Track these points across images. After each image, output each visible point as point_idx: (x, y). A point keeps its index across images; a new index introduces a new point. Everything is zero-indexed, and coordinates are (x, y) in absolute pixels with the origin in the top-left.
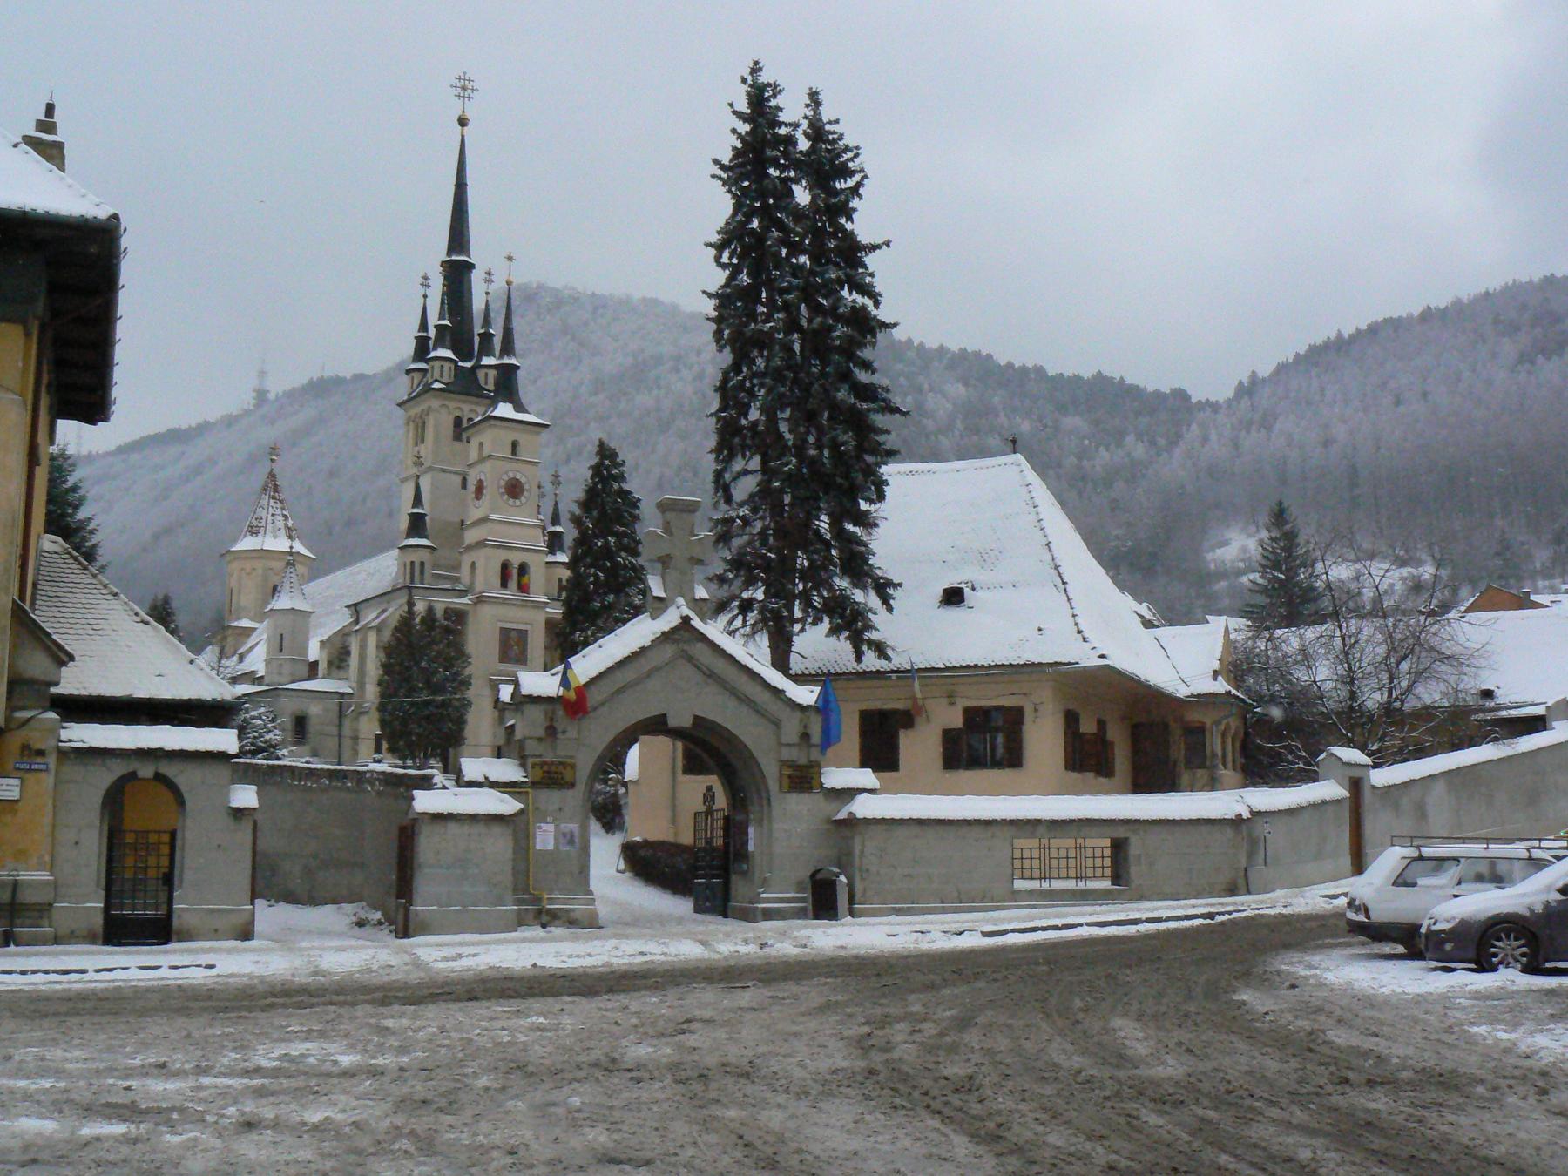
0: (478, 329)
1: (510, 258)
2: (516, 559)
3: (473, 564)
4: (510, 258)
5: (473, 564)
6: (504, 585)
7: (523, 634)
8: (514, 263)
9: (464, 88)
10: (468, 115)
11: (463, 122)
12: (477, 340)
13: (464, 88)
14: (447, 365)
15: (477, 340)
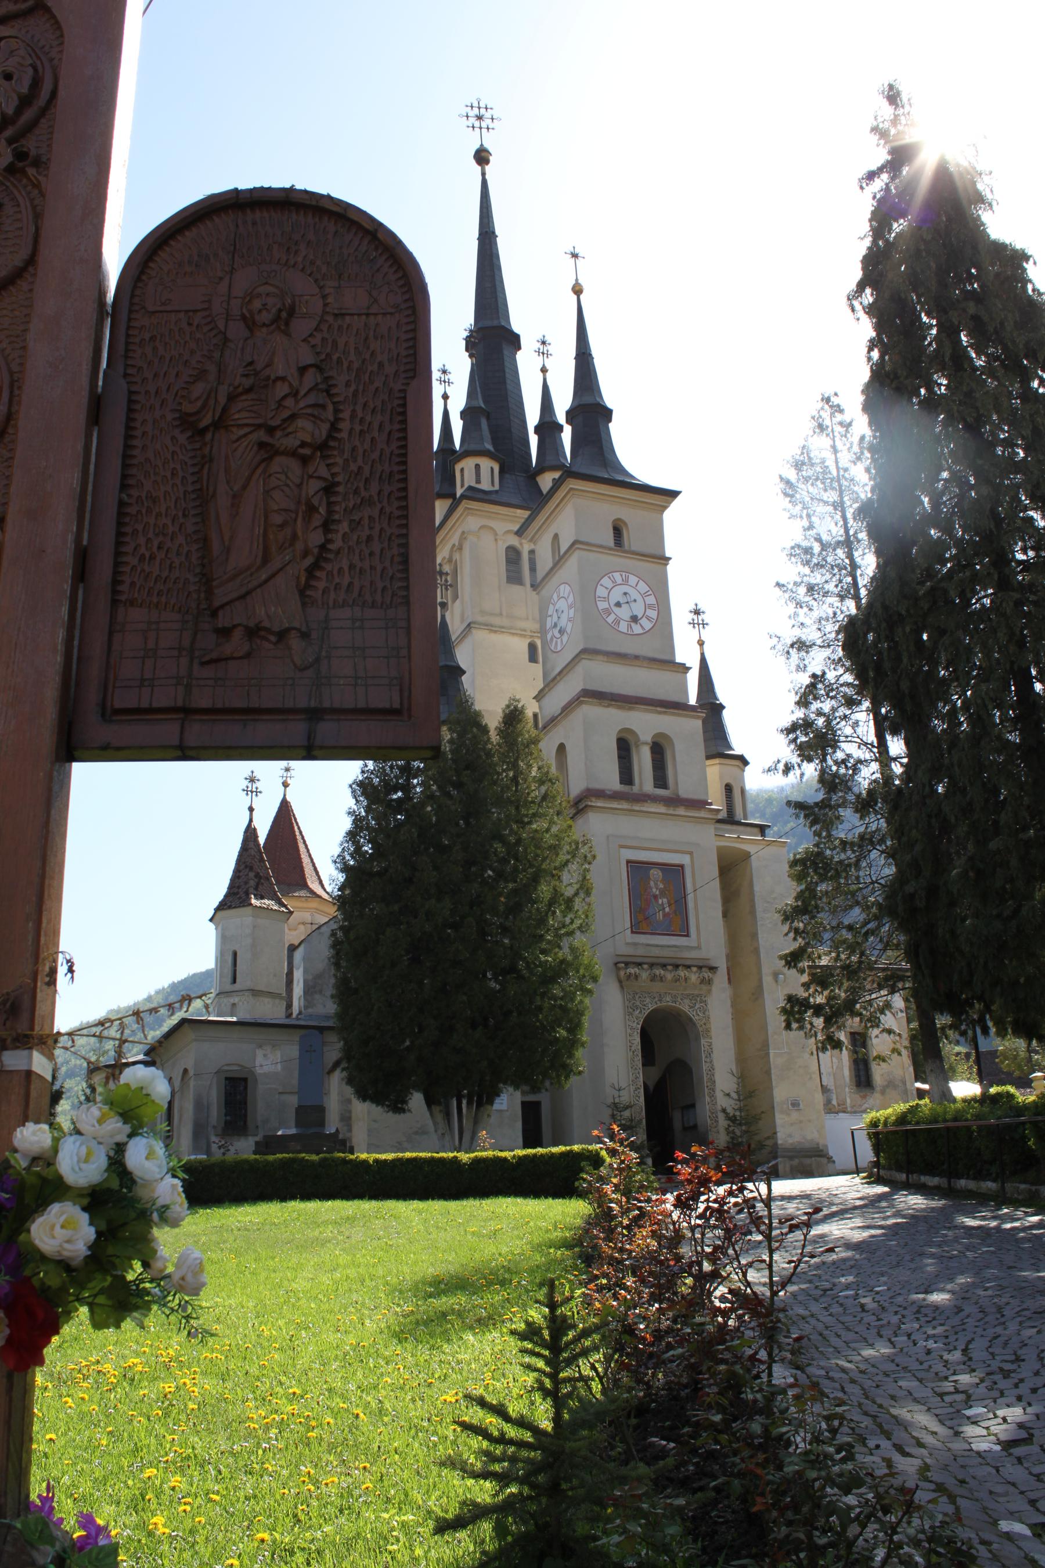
0: (533, 416)
1: (575, 256)
2: (646, 725)
3: (561, 748)
4: (575, 256)
5: (561, 748)
6: (627, 776)
7: (674, 873)
8: (579, 261)
9: (480, 117)
10: (486, 145)
11: (482, 157)
12: (534, 440)
13: (480, 117)
14: (487, 465)
15: (534, 440)
